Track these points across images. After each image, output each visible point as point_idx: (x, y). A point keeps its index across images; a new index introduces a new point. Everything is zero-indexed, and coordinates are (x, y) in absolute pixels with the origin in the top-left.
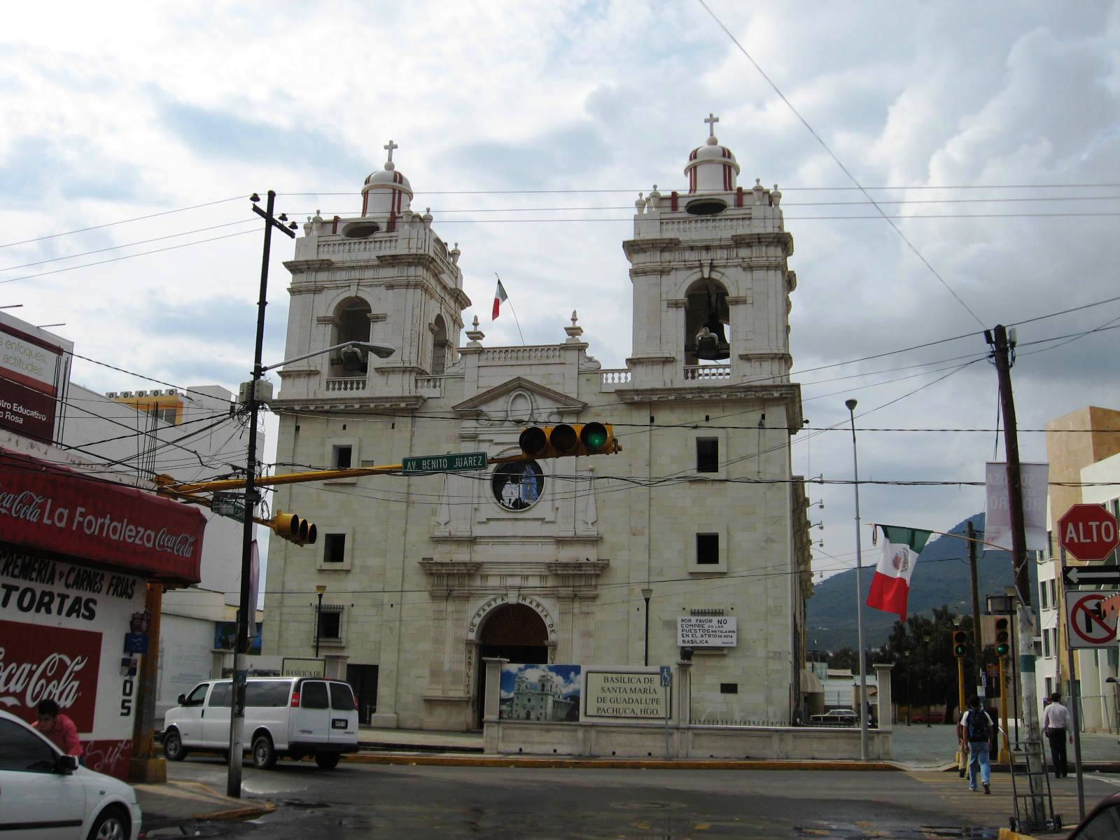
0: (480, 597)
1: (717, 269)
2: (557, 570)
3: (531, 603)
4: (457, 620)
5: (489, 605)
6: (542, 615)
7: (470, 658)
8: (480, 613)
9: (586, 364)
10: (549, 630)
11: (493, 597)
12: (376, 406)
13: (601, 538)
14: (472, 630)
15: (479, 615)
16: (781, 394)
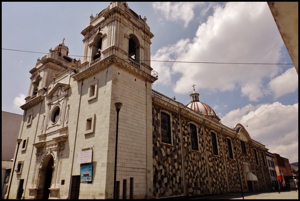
1: (101, 29)
5: (45, 156)
6: (54, 157)
10: (54, 162)
12: (35, 102)
13: (68, 127)
16: (110, 61)
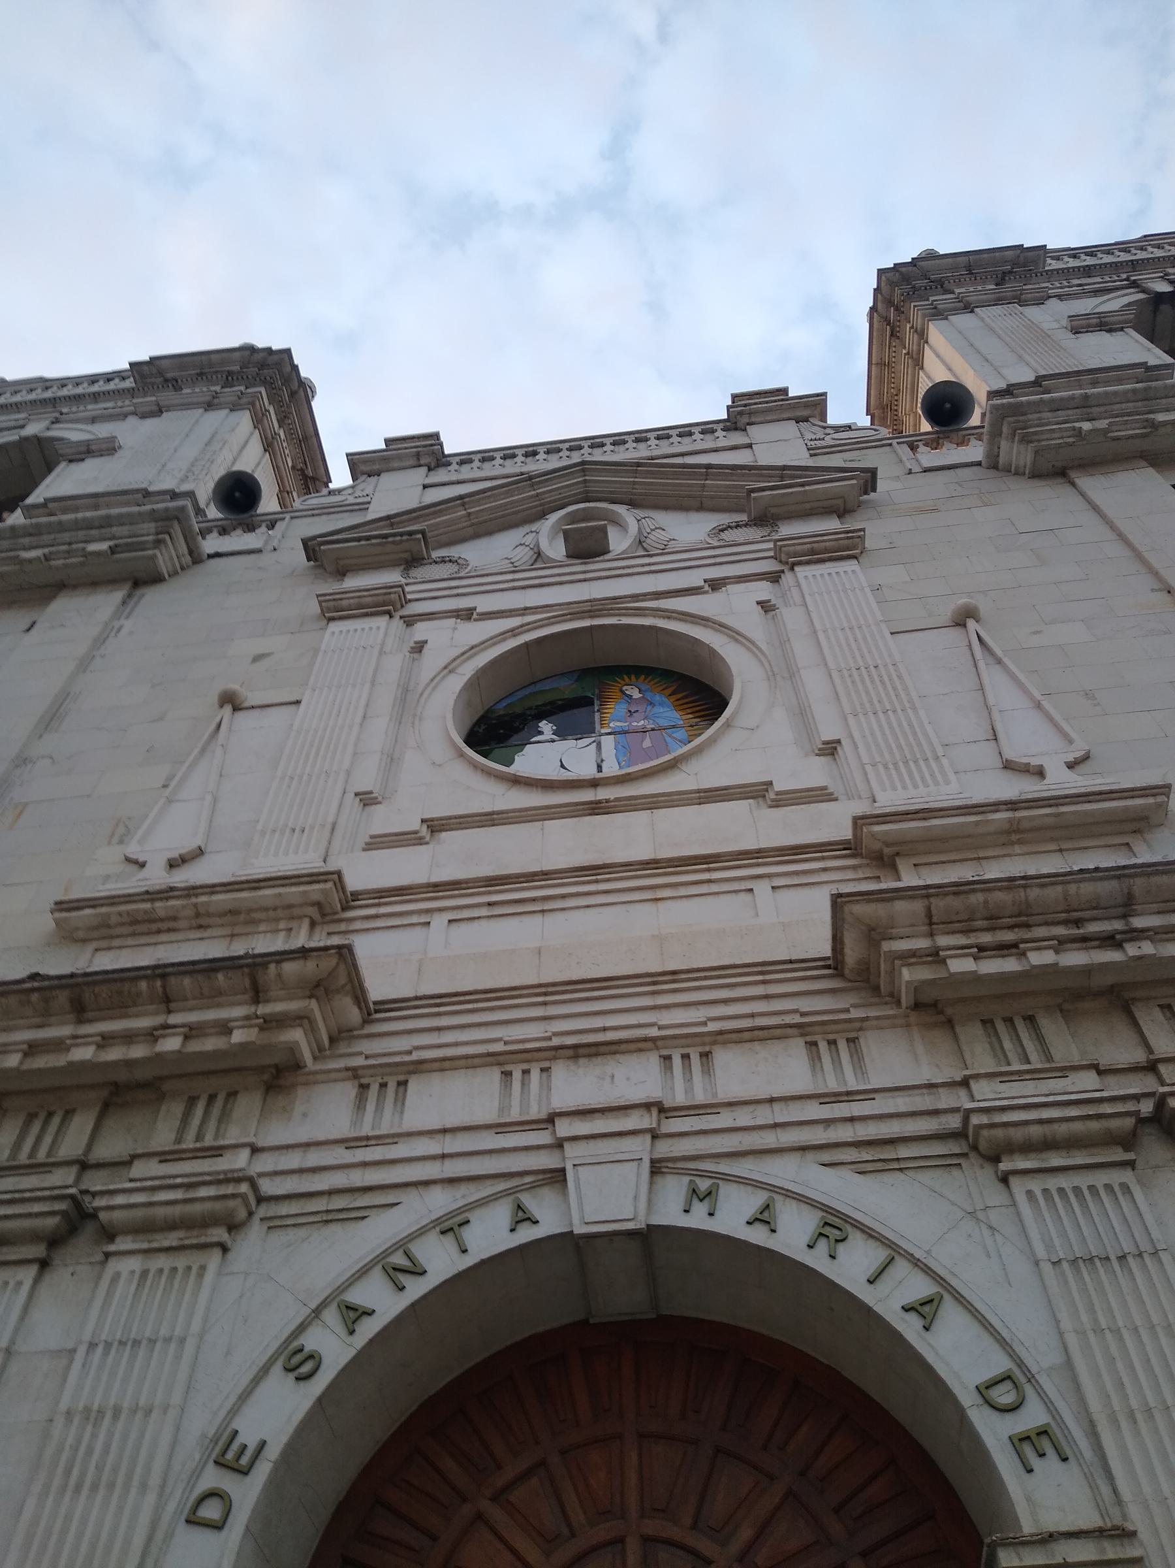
0: (329, 1219)
2: (935, 957)
3: (763, 1218)
8: (312, 1341)
9: (828, 438)
11: (440, 1201)
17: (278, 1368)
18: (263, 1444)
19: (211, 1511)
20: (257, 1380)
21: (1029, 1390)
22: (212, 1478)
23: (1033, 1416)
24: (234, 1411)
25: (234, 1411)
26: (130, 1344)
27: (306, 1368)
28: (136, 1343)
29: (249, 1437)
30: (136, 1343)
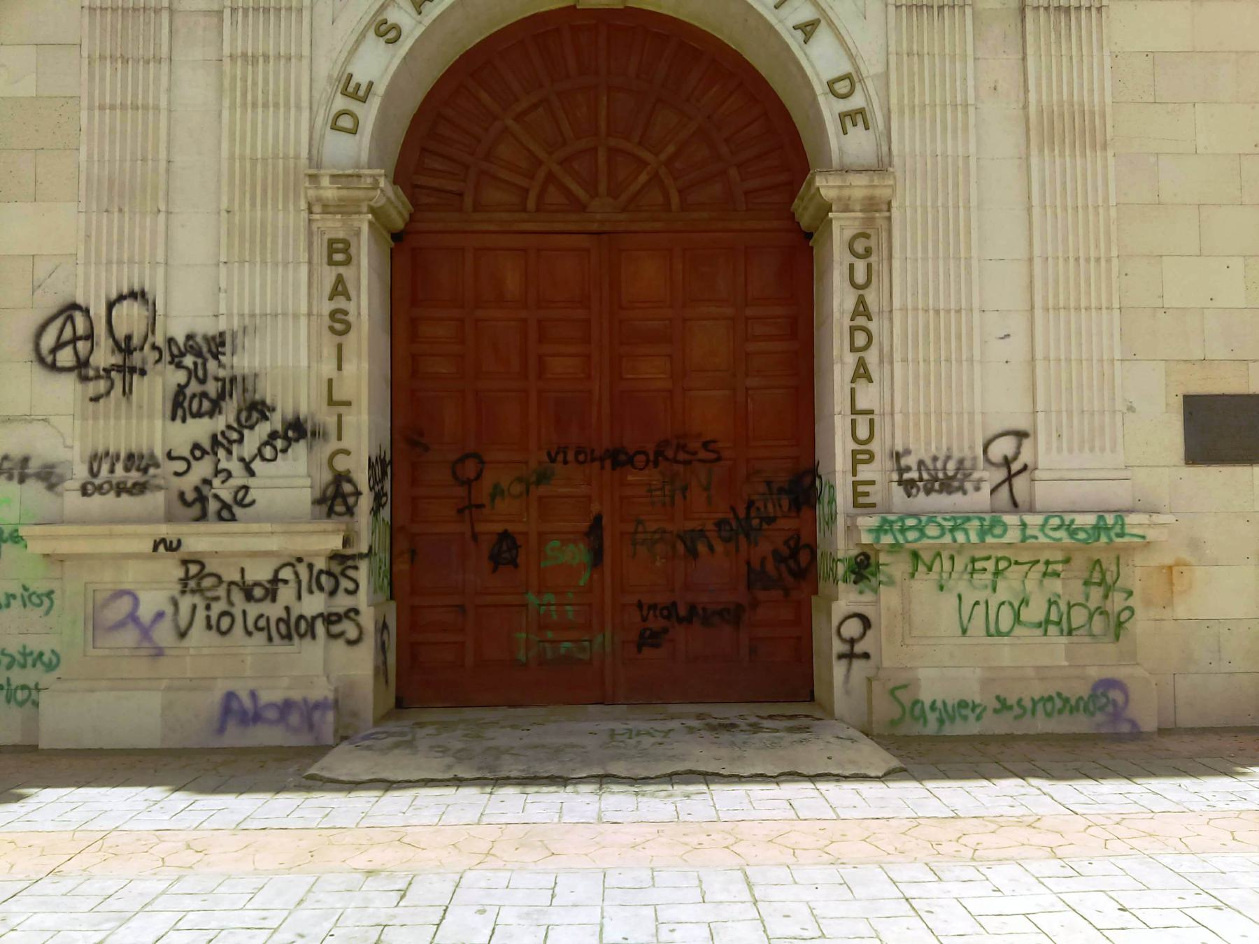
4: (249, 59)
7: (340, 289)
8: (393, 16)
14: (343, 123)
15: (387, 32)
17: (371, 34)
18: (371, 84)
19: (346, 122)
20: (358, 42)
21: (858, 87)
22: (340, 103)
23: (857, 101)
24: (347, 61)
25: (347, 61)
26: (261, 10)
27: (392, 35)
28: (267, 10)
29: (361, 76)
30: (267, 10)
